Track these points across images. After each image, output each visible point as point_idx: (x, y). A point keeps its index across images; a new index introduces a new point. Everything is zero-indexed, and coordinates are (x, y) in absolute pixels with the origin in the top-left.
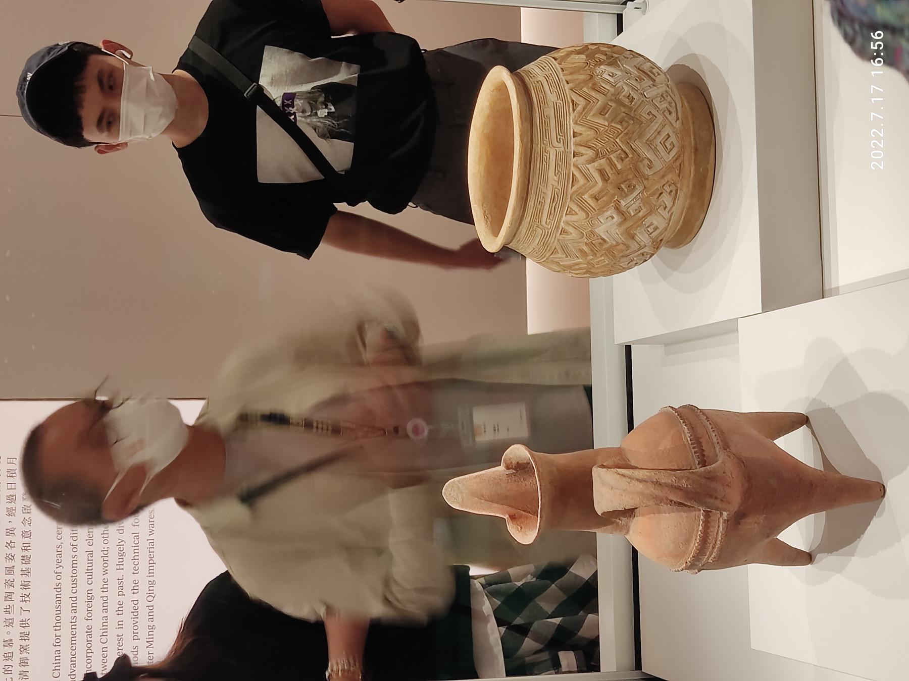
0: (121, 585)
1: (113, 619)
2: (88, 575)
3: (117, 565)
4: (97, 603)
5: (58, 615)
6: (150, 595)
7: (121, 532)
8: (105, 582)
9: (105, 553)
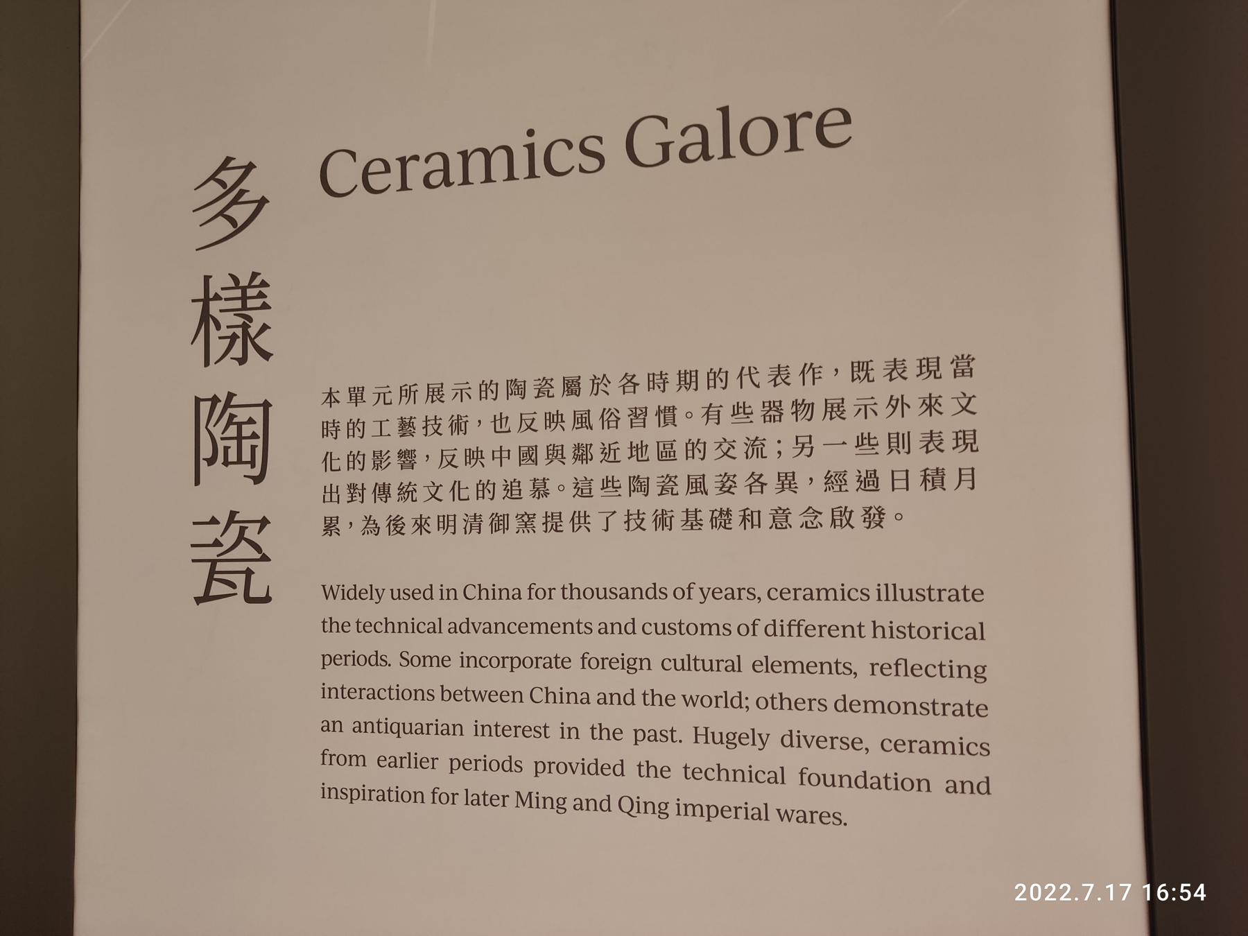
0: (659, 737)
1: (583, 716)
2: (683, 660)
3: (706, 729)
4: (618, 681)
5: (595, 593)
6: (636, 804)
7: (787, 741)
8: (667, 701)
9: (734, 701)
